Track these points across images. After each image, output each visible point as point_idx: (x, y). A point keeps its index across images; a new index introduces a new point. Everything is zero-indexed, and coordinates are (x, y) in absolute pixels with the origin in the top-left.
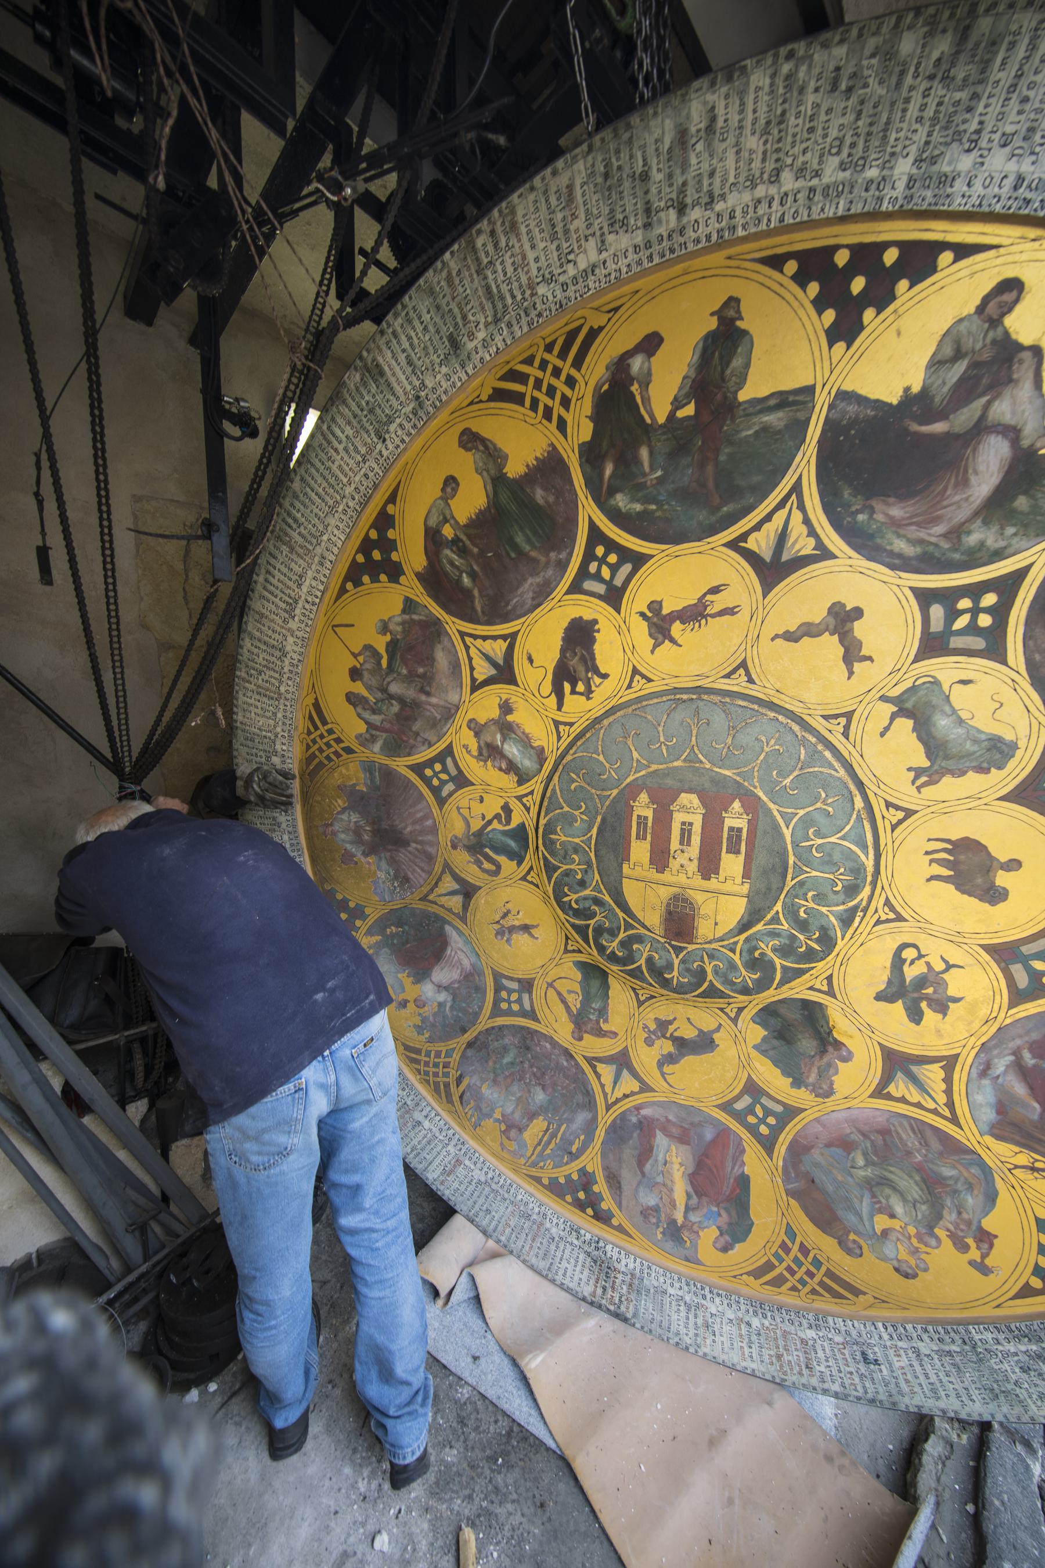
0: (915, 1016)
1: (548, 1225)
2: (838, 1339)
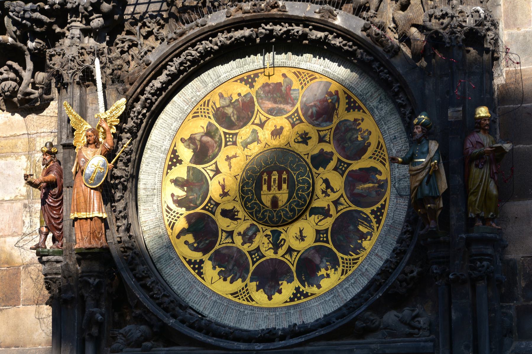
0: (310, 138)
1: (390, 224)
2: (392, 145)
